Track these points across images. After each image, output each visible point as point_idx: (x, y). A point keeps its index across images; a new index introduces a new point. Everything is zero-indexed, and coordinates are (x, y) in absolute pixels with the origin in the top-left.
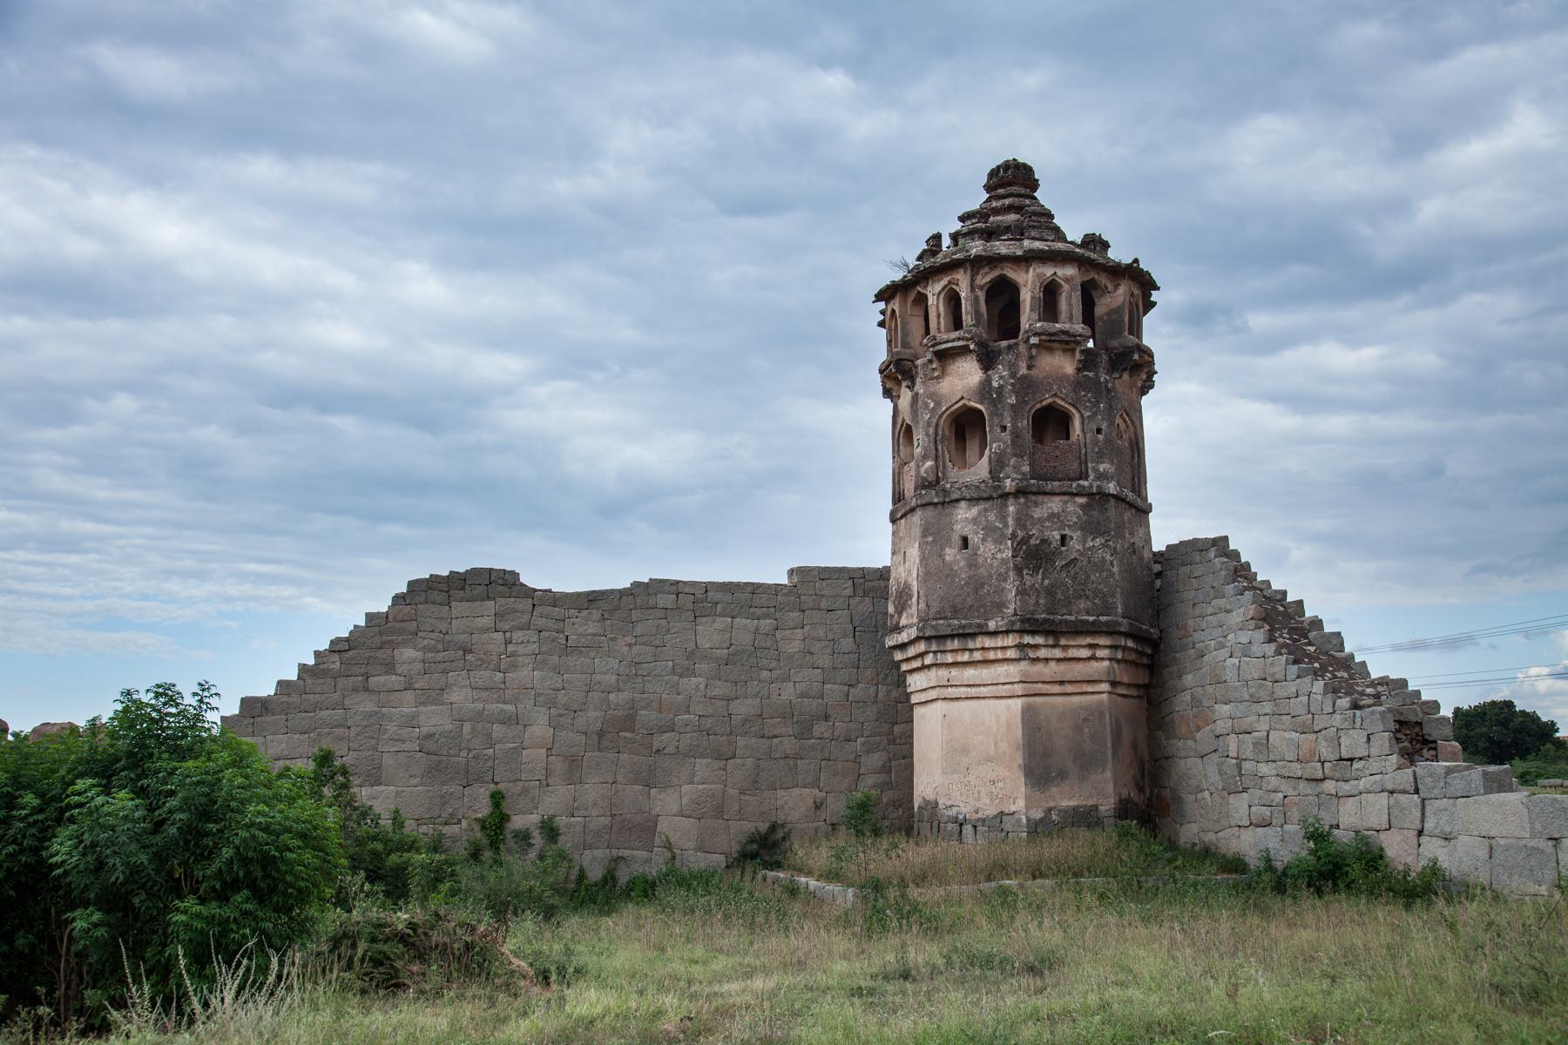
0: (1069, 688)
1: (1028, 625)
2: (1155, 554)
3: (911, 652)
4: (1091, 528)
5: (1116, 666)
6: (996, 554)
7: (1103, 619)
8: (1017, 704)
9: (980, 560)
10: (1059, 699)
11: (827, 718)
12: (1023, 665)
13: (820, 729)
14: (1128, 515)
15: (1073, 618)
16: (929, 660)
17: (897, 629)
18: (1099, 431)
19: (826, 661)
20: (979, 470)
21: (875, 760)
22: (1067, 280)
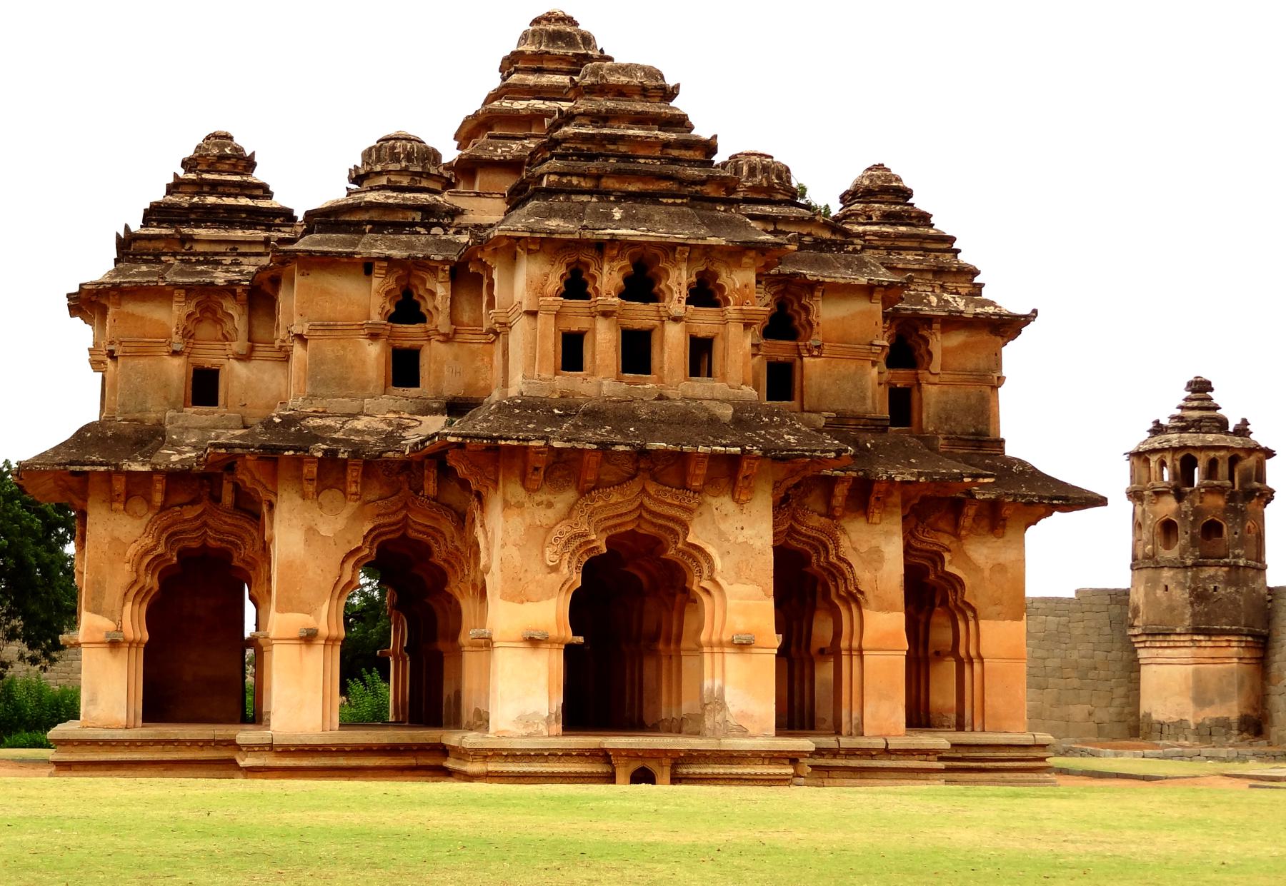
1: (1197, 631)
3: (1140, 639)
4: (1228, 583)
5: (1241, 649)
6: (1181, 596)
7: (1234, 627)
9: (1174, 598)
10: (1212, 666)
11: (1095, 669)
12: (1194, 649)
13: (1092, 674)
14: (1251, 573)
15: (1218, 627)
16: (1148, 644)
17: (1132, 626)
18: (1236, 533)
19: (1094, 639)
21: (1121, 691)
22: (1221, 458)
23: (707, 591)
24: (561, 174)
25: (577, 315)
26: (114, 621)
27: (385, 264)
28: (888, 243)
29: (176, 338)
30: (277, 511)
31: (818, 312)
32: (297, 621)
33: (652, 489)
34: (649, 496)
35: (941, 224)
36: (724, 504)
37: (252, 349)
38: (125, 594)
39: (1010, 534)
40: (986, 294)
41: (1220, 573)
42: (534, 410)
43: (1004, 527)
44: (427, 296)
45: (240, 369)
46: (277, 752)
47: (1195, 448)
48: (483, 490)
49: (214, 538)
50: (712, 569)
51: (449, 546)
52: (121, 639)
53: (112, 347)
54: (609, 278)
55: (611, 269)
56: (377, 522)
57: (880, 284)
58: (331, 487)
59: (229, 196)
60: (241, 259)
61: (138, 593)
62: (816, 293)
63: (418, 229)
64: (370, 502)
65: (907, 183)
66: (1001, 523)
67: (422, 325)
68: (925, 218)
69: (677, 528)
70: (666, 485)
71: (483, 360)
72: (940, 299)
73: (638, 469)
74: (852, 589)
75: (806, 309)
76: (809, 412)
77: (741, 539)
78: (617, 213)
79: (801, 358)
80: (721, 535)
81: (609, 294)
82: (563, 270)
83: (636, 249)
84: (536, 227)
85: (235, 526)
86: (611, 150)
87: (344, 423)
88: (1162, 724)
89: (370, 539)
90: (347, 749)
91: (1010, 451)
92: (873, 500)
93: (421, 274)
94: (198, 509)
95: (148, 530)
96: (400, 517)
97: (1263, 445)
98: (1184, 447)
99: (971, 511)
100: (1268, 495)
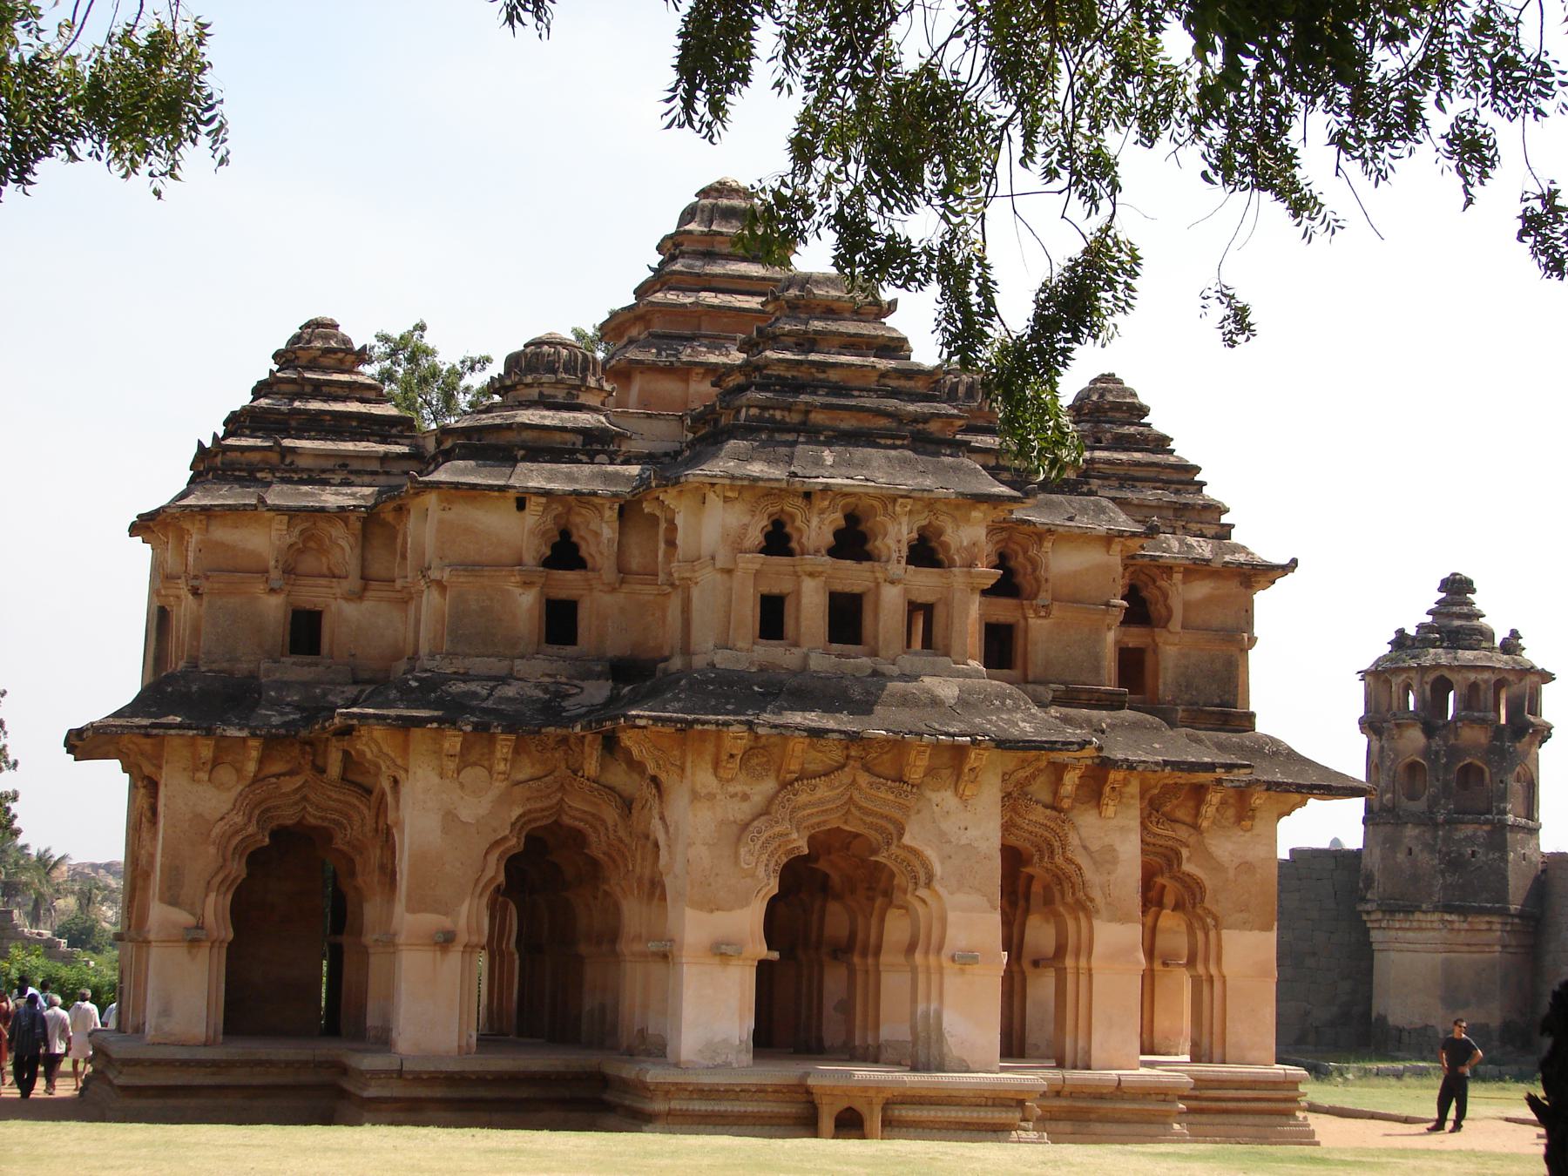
0: (1473, 949)
1: (1449, 909)
2: (1543, 855)
6: (1425, 859)
8: (1440, 957)
10: (1467, 956)
11: (1314, 954)
12: (1444, 933)
16: (1384, 924)
17: (1364, 900)
18: (1502, 782)
20: (1420, 806)
22: (1486, 682)
23: (924, 901)
24: (763, 408)
25: (778, 574)
26: (194, 915)
27: (543, 500)
28: (1121, 471)
29: (275, 574)
30: (405, 789)
31: (1047, 567)
32: (430, 921)
33: (864, 779)
34: (859, 789)
35: (1184, 449)
36: (945, 798)
37: (365, 589)
38: (209, 883)
39: (1259, 826)
40: (1236, 537)
41: (1479, 833)
42: (731, 686)
43: (1253, 818)
44: (589, 537)
45: (351, 610)
46: (406, 1080)
47: (1450, 668)
48: (663, 777)
49: (314, 817)
50: (930, 877)
51: (612, 837)
52: (203, 937)
53: (196, 583)
54: (817, 529)
55: (822, 521)
56: (529, 807)
57: (1121, 534)
58: (475, 764)
59: (336, 399)
60: (353, 478)
61: (222, 881)
62: (1045, 544)
63: (580, 457)
64: (519, 783)
65: (1143, 399)
66: (1250, 813)
67: (583, 572)
68: (1161, 443)
69: (891, 827)
70: (879, 777)
71: (653, 615)
72: (1182, 542)
73: (848, 757)
74: (1081, 895)
75: (1035, 565)
76: (1034, 682)
77: (964, 841)
78: (828, 456)
79: (1026, 619)
80: (943, 837)
81: (817, 551)
82: (765, 523)
83: (849, 500)
84: (738, 472)
85: (340, 801)
86: (820, 380)
87: (492, 689)
88: (1400, 1030)
89: (519, 824)
90: (489, 1077)
91: (1262, 727)
92: (1107, 789)
93: (584, 511)
94: (298, 781)
95: (238, 805)
96: (554, 801)
97: (1539, 665)
98: (1438, 666)
99: (1214, 798)
100: (1544, 733)
